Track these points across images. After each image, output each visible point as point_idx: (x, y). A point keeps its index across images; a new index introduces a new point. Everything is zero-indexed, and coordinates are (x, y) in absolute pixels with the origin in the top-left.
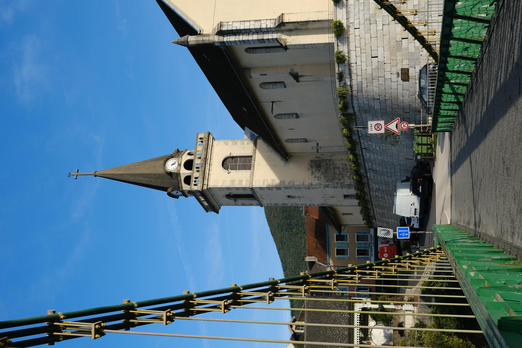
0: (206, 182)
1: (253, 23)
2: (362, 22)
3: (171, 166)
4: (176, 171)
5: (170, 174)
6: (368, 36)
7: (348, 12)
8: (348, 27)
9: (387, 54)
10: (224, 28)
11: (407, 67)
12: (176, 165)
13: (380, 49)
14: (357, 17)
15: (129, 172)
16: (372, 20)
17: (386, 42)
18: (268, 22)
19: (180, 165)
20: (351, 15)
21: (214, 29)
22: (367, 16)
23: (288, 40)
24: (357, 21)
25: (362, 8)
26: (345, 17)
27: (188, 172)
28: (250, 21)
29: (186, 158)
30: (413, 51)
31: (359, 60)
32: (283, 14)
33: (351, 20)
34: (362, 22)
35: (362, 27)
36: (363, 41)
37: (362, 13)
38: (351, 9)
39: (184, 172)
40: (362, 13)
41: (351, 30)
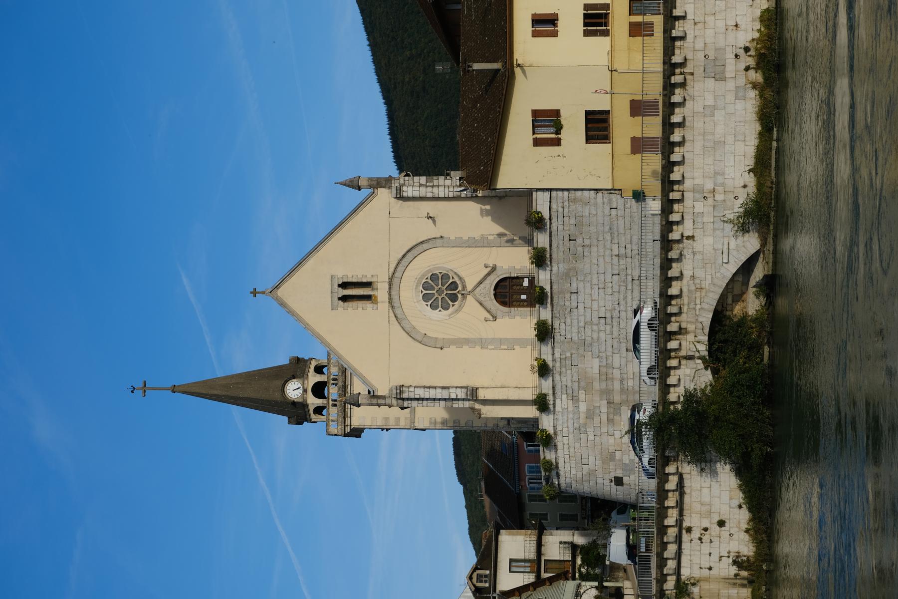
0: (348, 422)
1: (439, 390)
2: (571, 431)
3: (293, 390)
4: (301, 400)
5: (294, 403)
6: (577, 445)
7: (555, 420)
8: (556, 434)
9: (598, 463)
10: (405, 396)
11: (621, 476)
12: (301, 391)
13: (592, 459)
14: (565, 425)
15: (229, 394)
16: (582, 429)
17: (598, 452)
18: (459, 390)
19: (305, 391)
20: (559, 423)
21: (391, 390)
22: (576, 425)
23: (482, 411)
24: (565, 430)
25: (571, 416)
26: (552, 424)
27: (319, 402)
28: (435, 388)
29: (313, 378)
30: (627, 462)
31: (568, 467)
32: (477, 389)
33: (559, 428)
34: (571, 431)
35: (571, 436)
36: (572, 450)
37: (570, 422)
38: (559, 416)
39: (313, 401)
40: (570, 422)
41: (559, 438)
